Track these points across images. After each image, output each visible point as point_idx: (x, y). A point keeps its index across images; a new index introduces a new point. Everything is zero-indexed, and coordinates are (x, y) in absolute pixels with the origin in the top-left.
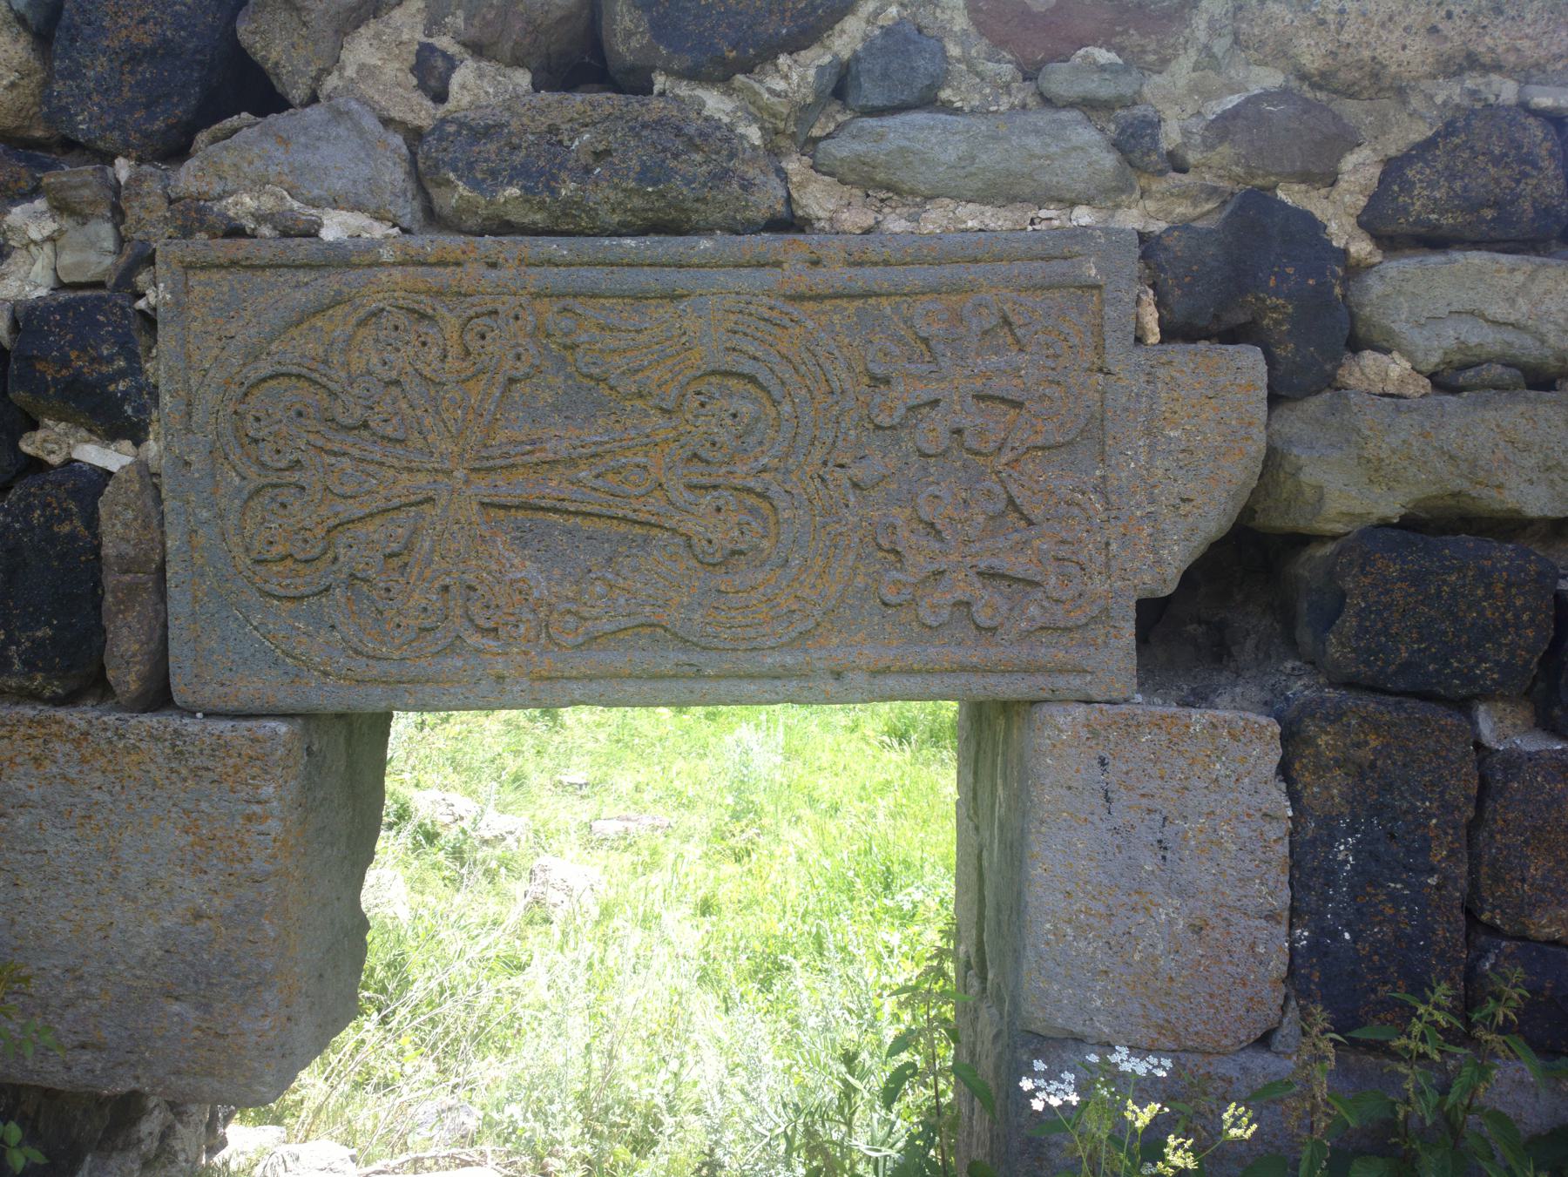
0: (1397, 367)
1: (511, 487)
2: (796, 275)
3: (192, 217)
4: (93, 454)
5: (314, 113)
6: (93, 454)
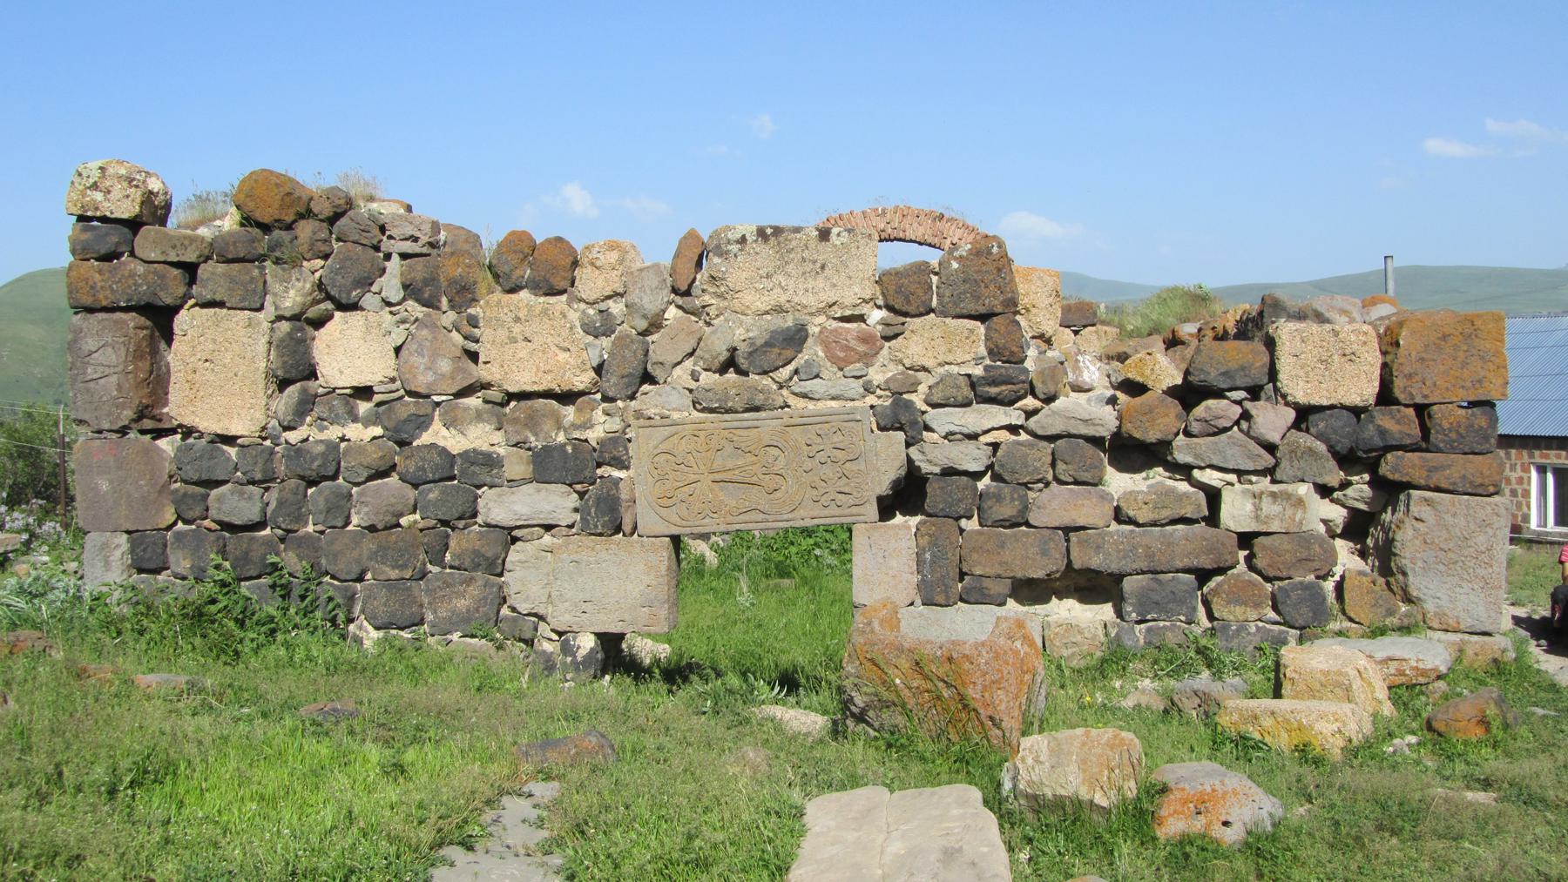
0: (935, 436)
1: (718, 477)
2: (786, 420)
3: (639, 415)
4: (616, 474)
5: (667, 388)
6: (616, 474)
